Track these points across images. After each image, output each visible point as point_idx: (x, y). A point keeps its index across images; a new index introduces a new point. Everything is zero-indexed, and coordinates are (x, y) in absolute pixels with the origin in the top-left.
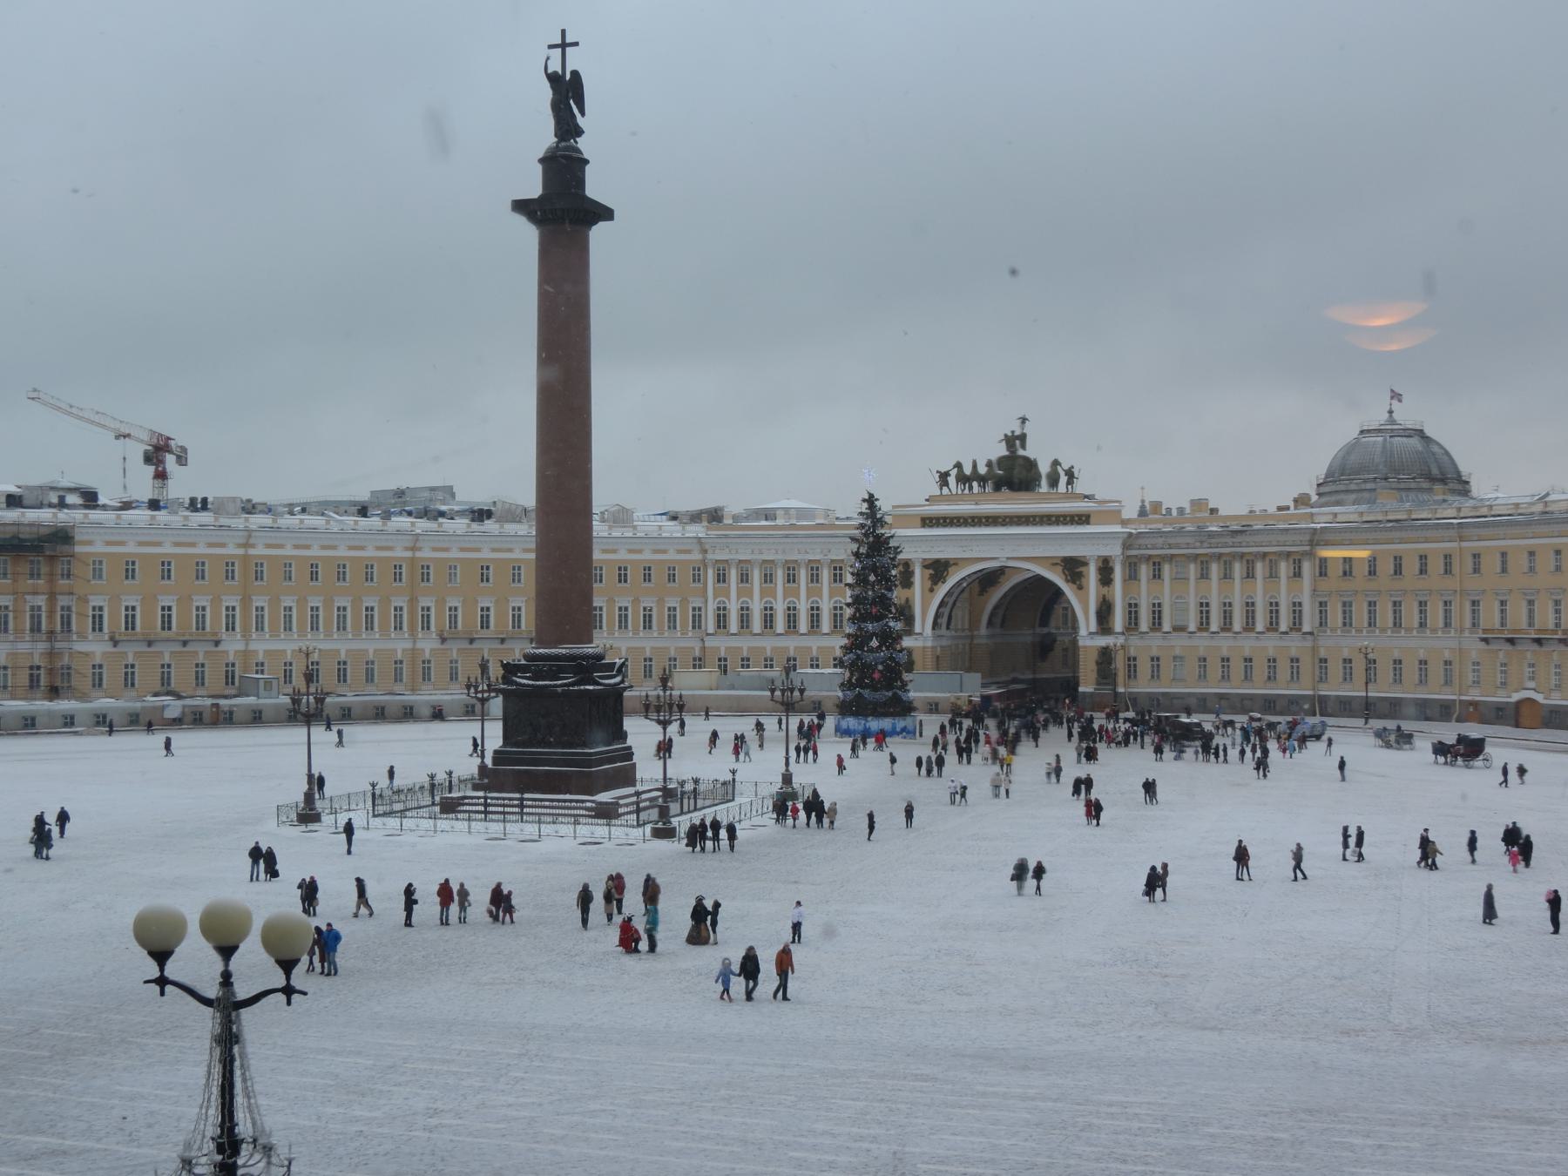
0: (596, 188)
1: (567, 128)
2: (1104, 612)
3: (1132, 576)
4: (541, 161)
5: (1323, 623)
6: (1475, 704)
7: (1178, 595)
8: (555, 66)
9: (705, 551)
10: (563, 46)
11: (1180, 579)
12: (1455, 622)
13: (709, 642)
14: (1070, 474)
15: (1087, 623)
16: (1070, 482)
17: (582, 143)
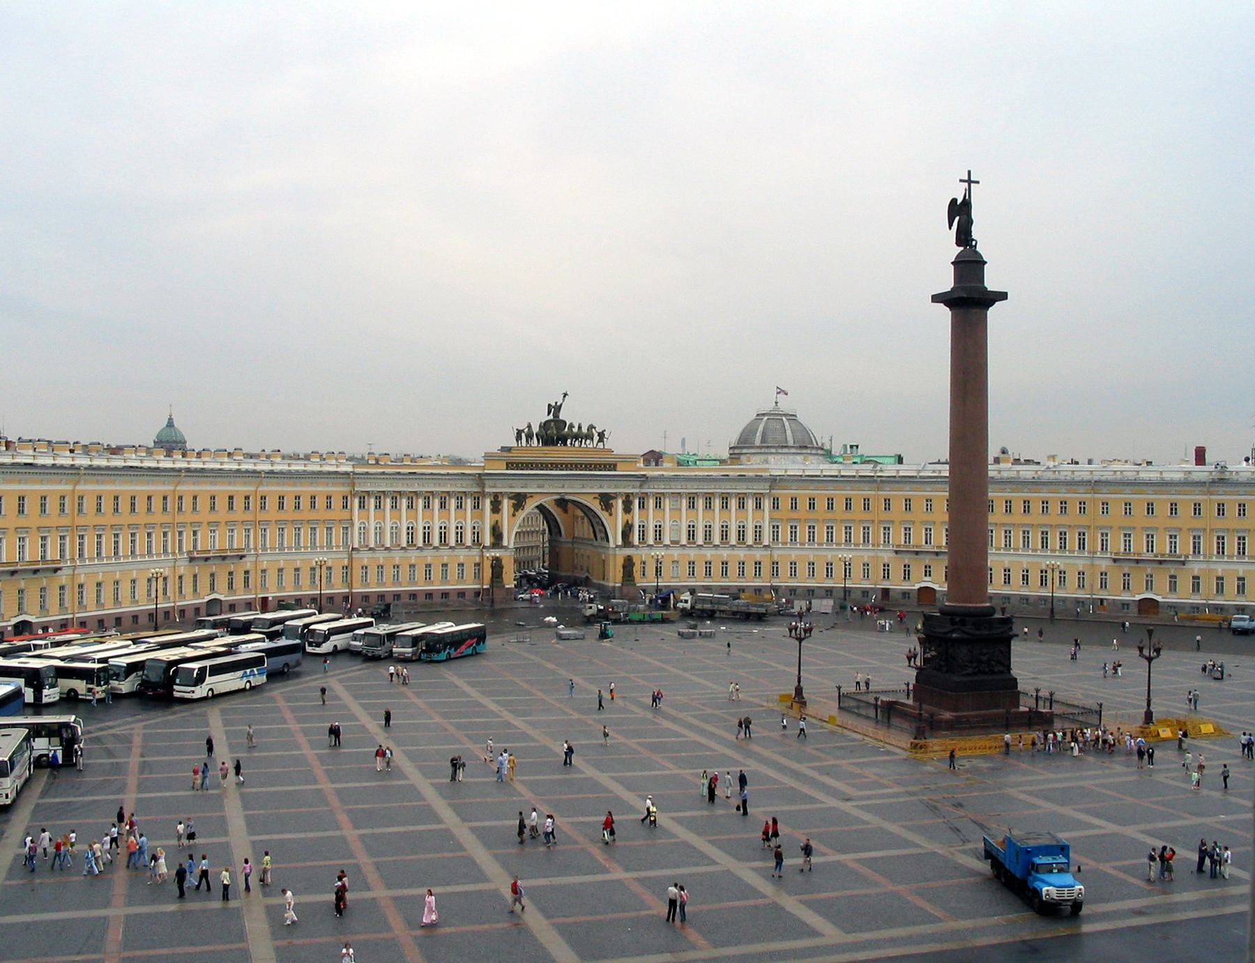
0: (991, 282)
1: (964, 237)
3: (642, 506)
5: (775, 537)
7: (673, 520)
9: (353, 485)
13: (355, 555)
14: (601, 436)
16: (601, 440)
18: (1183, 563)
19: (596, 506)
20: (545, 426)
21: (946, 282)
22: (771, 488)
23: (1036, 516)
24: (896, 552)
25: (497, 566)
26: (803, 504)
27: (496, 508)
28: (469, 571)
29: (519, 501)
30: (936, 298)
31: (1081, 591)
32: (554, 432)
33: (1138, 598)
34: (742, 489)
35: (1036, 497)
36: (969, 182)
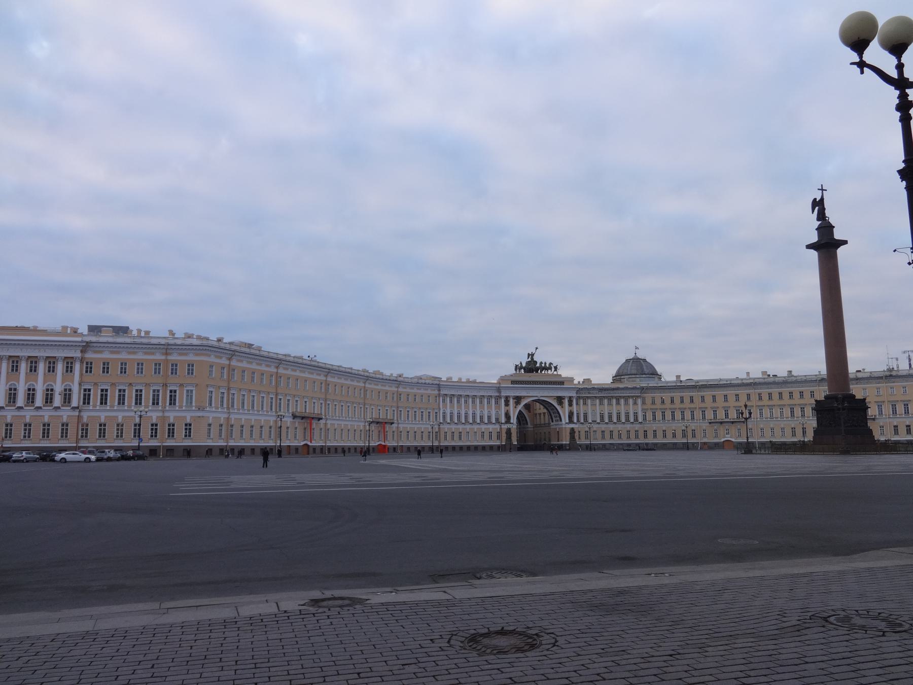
1: (822, 216)
3: (577, 404)
6: (705, 443)
7: (593, 410)
11: (594, 405)
14: (556, 368)
15: (565, 419)
16: (556, 370)
19: (555, 403)
20: (528, 363)
21: (814, 238)
23: (786, 400)
25: (509, 432)
26: (658, 401)
27: (507, 404)
28: (494, 436)
30: (809, 247)
32: (531, 367)
35: (786, 391)
36: (822, 190)
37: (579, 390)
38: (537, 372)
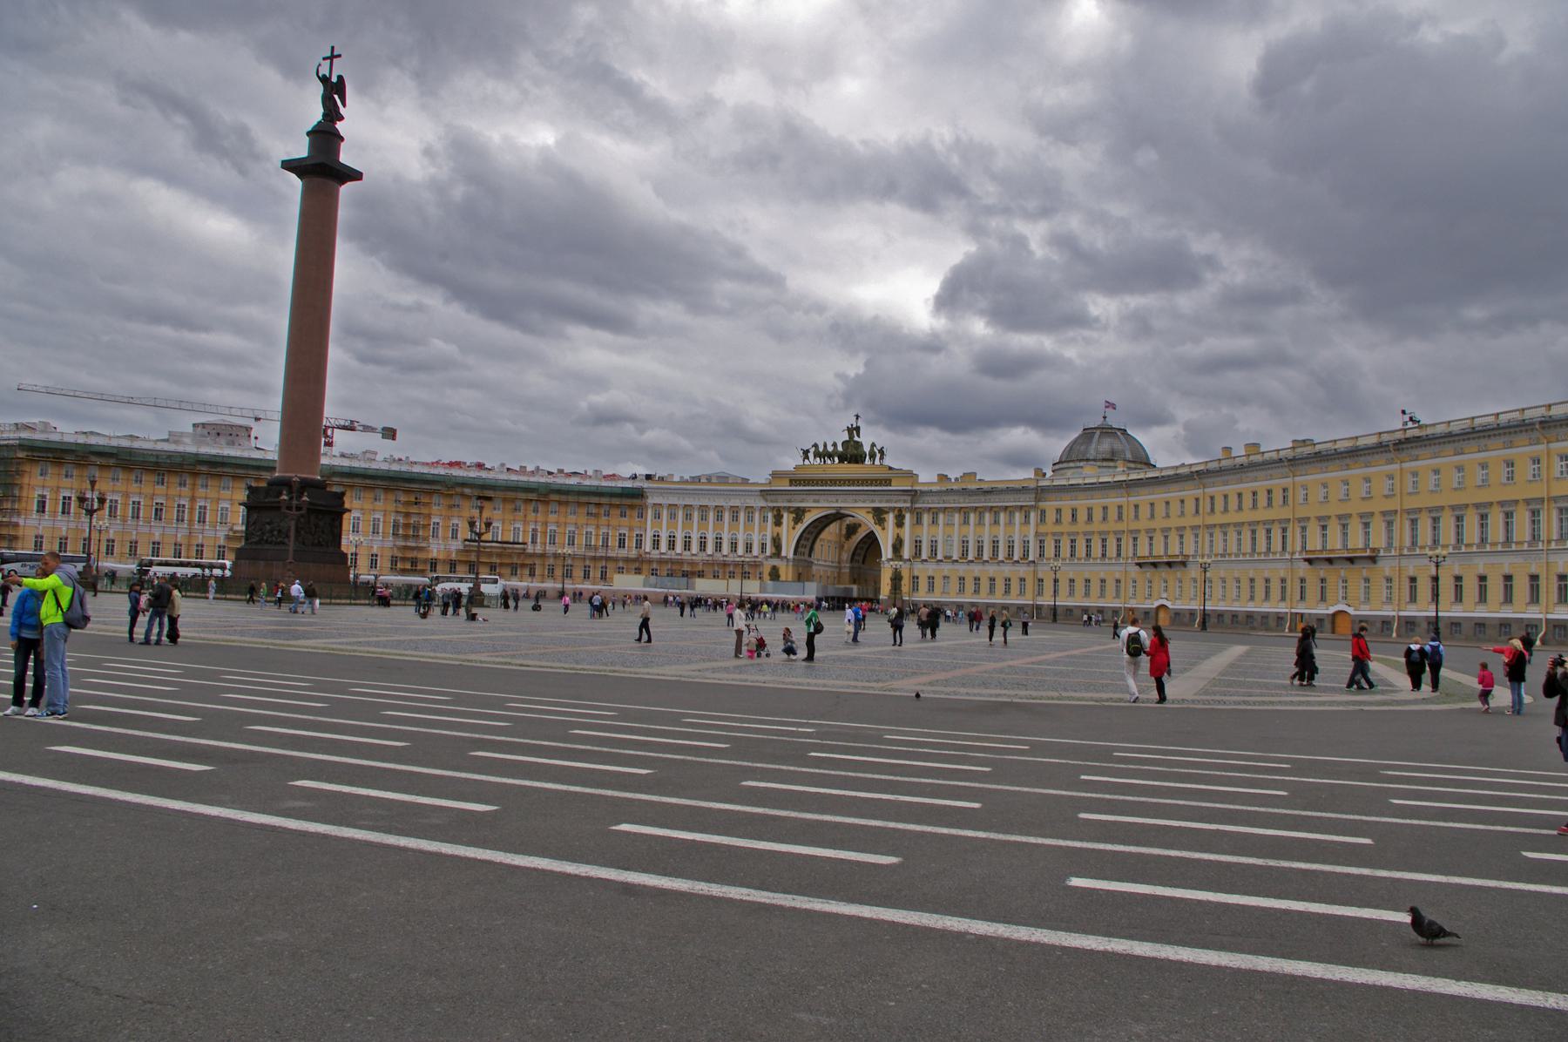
1: (332, 113)
2: (898, 546)
4: (309, 134)
7: (946, 533)
8: (324, 71)
10: (332, 57)
11: (949, 524)
12: (1123, 554)
14: (881, 451)
15: (887, 552)
17: (339, 125)
18: (1373, 559)
22: (1037, 500)
24: (1140, 565)
27: (778, 523)
29: (799, 514)
31: (1282, 604)
32: (852, 453)
33: (1332, 610)
34: (1010, 501)
37: (914, 495)
38: (863, 461)
